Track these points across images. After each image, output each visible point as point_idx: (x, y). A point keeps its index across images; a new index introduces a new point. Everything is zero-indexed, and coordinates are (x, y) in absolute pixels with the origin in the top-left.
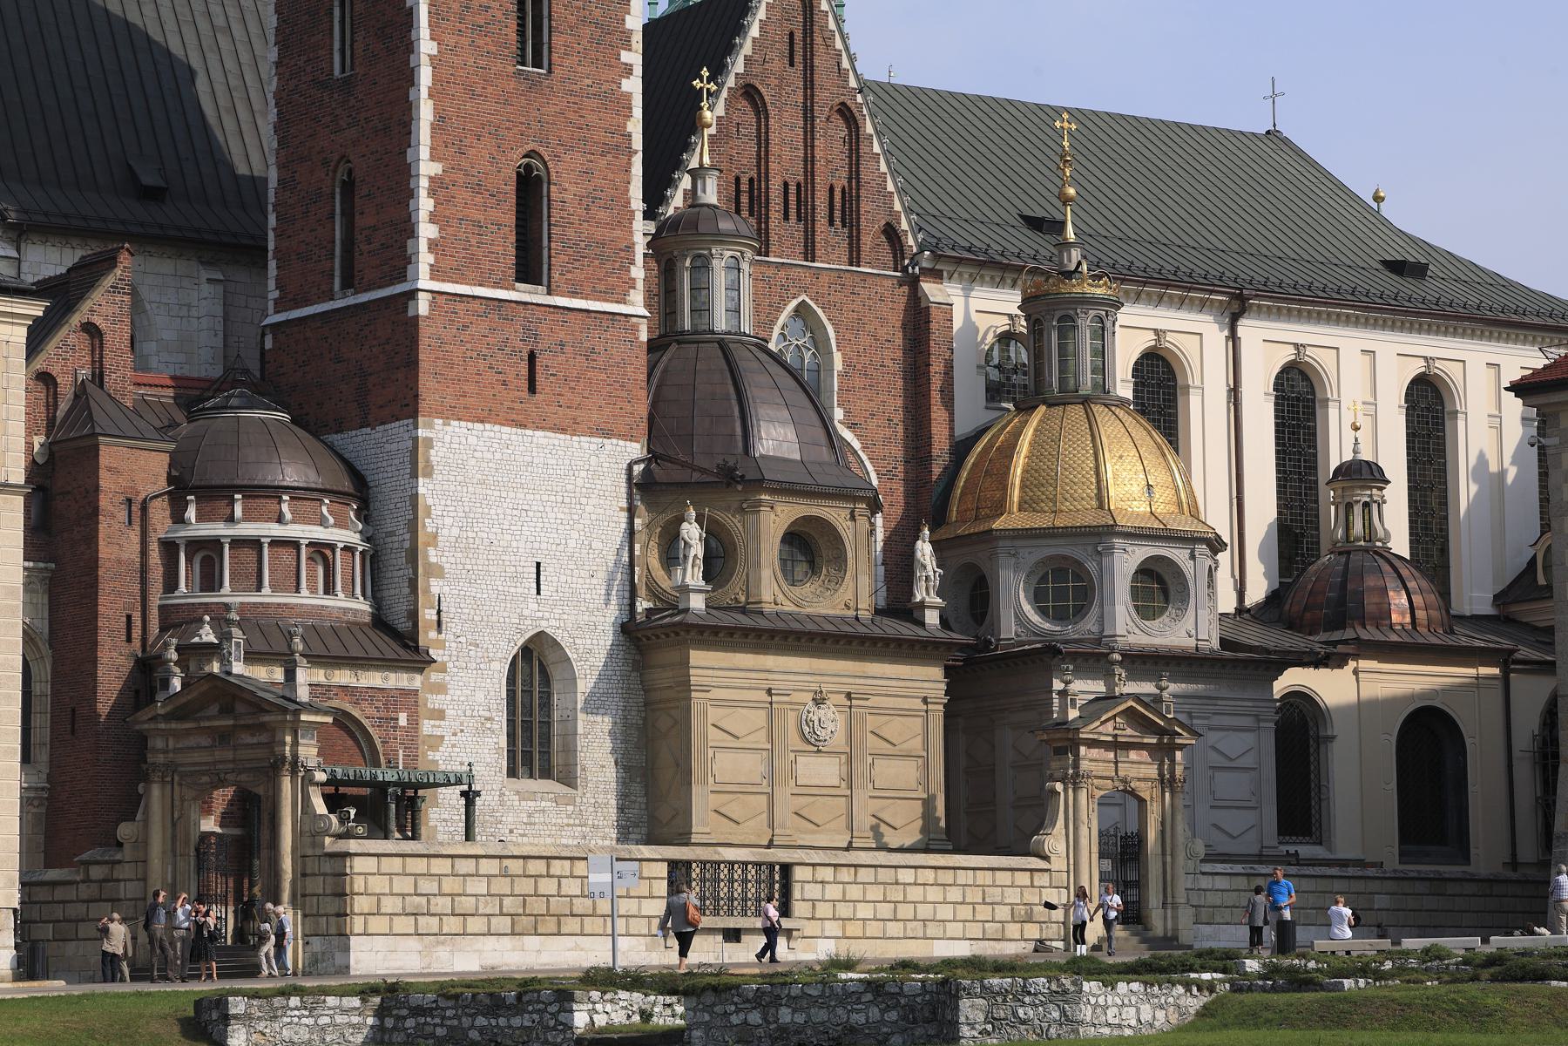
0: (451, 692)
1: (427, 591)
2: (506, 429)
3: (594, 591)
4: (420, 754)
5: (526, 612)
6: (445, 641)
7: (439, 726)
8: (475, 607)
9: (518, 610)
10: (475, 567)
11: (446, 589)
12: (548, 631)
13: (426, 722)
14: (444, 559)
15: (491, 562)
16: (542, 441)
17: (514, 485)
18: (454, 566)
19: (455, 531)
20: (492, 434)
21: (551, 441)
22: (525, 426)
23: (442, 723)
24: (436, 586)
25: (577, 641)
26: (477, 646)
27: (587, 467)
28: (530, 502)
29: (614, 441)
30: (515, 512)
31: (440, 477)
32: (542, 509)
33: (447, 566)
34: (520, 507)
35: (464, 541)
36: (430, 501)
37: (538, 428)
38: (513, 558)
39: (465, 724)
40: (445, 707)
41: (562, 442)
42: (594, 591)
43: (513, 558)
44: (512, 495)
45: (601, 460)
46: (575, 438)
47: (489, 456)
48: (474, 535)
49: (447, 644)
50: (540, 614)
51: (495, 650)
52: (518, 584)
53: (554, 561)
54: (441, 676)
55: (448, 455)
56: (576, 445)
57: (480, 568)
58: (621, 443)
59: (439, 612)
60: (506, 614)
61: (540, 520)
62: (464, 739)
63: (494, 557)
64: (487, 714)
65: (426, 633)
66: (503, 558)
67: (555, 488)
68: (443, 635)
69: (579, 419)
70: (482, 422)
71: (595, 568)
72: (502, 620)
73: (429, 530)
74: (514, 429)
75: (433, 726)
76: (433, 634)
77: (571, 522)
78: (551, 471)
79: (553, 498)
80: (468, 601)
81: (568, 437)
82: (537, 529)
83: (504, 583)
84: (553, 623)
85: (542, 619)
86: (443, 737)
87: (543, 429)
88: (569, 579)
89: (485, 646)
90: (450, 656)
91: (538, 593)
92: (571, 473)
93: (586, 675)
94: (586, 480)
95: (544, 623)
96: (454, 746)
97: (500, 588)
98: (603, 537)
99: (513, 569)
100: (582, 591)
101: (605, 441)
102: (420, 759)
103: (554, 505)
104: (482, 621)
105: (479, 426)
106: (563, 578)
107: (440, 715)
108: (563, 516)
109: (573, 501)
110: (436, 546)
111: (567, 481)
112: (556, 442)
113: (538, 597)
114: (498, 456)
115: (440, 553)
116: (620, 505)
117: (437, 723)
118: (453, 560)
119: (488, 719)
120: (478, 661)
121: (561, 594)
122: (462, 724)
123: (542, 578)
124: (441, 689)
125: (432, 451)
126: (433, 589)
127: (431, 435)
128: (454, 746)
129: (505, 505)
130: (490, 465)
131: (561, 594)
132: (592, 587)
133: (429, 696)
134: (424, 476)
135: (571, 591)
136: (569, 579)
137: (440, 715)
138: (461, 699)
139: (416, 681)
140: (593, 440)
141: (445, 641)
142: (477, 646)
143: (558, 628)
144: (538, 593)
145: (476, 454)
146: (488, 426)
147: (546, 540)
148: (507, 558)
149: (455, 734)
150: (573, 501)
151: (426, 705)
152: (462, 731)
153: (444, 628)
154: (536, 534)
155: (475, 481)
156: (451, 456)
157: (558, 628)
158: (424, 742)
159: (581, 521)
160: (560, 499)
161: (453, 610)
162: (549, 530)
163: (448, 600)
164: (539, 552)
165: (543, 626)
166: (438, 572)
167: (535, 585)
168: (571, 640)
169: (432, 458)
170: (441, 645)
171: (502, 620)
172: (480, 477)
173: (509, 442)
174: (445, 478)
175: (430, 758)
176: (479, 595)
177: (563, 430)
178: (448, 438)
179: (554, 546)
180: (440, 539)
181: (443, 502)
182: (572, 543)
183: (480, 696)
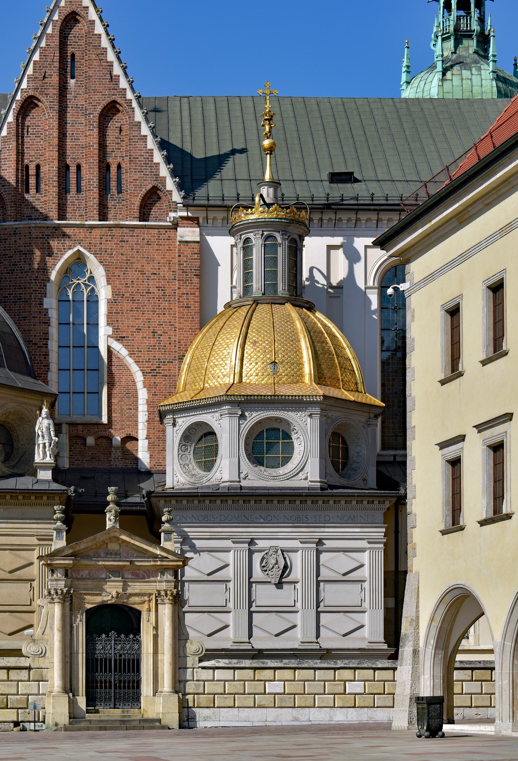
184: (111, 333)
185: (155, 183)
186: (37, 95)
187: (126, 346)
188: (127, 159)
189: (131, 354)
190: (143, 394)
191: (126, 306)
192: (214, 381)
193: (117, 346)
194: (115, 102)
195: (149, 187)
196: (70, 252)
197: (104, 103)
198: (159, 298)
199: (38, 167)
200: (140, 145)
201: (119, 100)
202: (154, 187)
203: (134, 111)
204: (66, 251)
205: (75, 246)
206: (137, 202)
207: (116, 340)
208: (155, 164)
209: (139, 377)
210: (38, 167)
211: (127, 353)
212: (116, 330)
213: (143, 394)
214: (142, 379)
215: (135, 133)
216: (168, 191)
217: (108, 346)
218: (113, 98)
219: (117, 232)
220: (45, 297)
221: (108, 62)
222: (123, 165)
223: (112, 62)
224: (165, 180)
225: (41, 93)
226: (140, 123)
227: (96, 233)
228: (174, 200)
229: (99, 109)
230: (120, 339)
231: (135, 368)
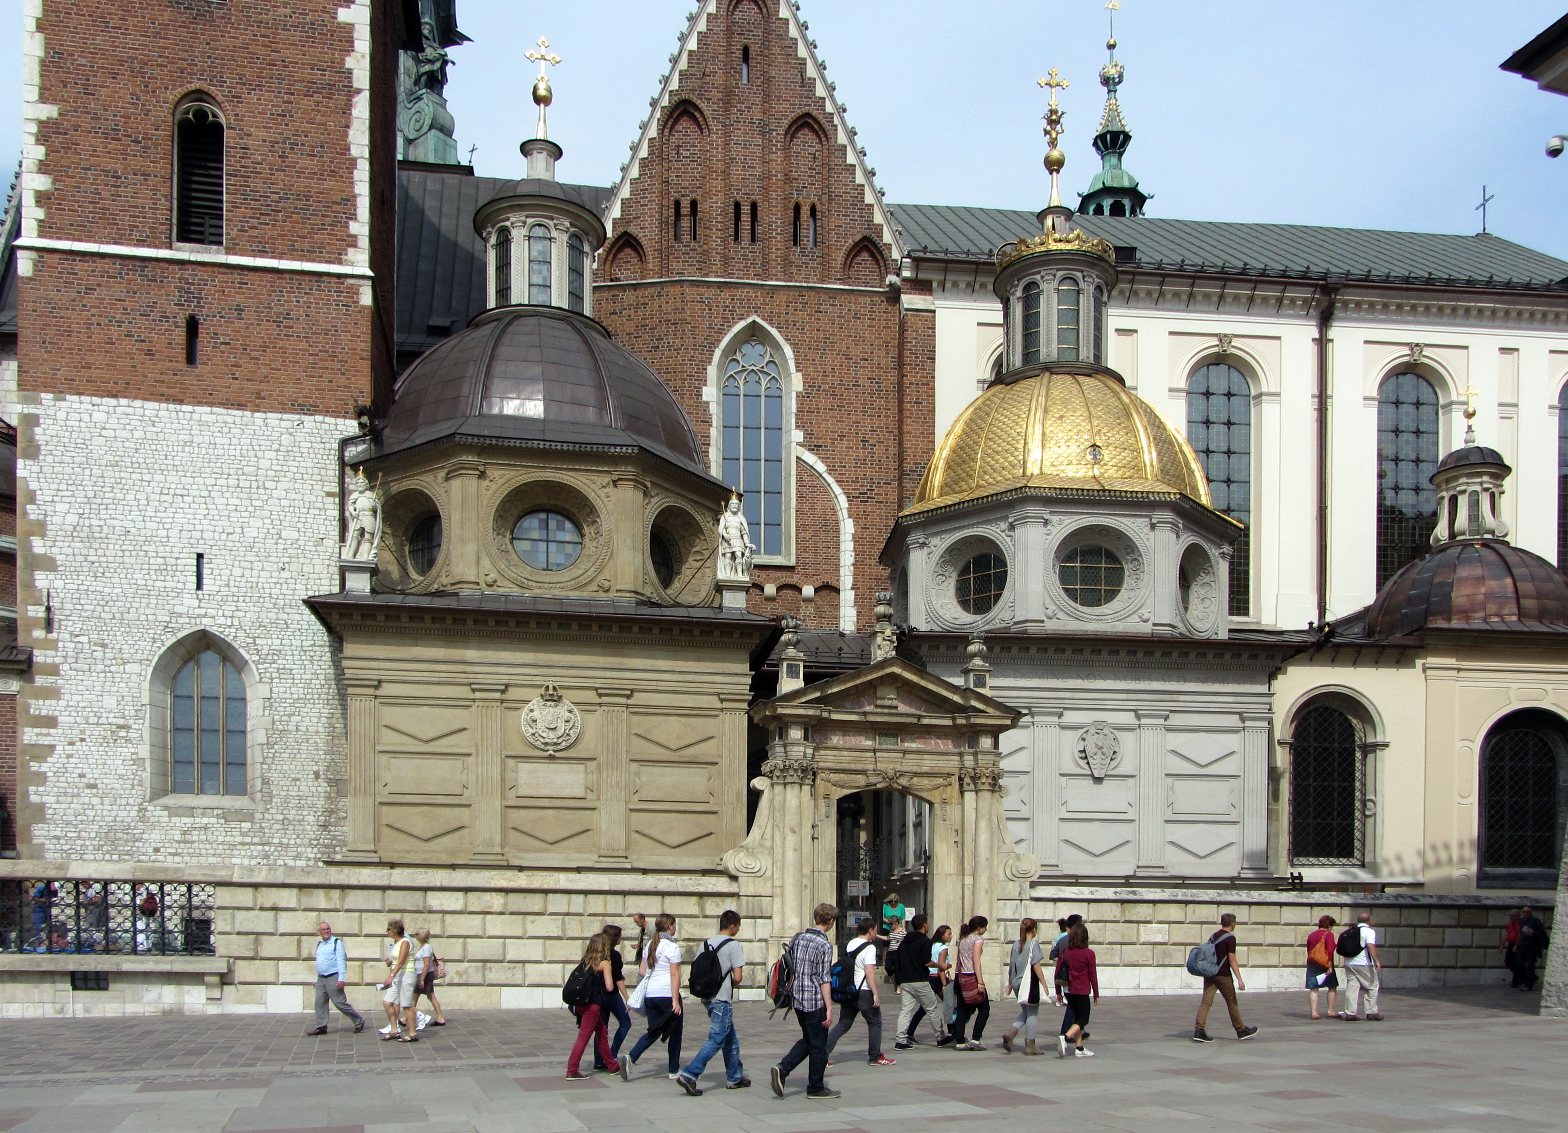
0: (67, 697)
1: (30, 585)
2: (155, 405)
3: (285, 586)
4: (18, 764)
5: (178, 609)
6: (57, 641)
7: (48, 735)
8: (102, 603)
9: (167, 607)
10: (104, 559)
11: (59, 583)
12: (214, 630)
13: (27, 730)
14: (54, 550)
15: (127, 553)
16: (205, 418)
17: (163, 467)
18: (71, 558)
19: (72, 519)
20: (130, 410)
21: (220, 418)
22: (181, 402)
23: (52, 731)
24: (42, 580)
25: (258, 641)
26: (104, 646)
27: (275, 447)
28: (187, 487)
29: (319, 418)
30: (164, 498)
31: (49, 459)
32: (206, 494)
33: (58, 557)
34: (171, 491)
35: (86, 529)
36: (33, 486)
37: (200, 403)
38: (161, 549)
39: (88, 733)
40: (57, 713)
41: (238, 420)
42: (285, 586)
43: (161, 549)
44: (159, 477)
45: (298, 439)
46: (257, 415)
47: (125, 434)
48: (102, 523)
49: (60, 644)
50: (203, 611)
51: (132, 651)
52: (169, 578)
53: (223, 552)
54: (51, 679)
55: (61, 434)
56: (259, 422)
57: (110, 559)
58: (328, 419)
59: (48, 609)
60: (148, 611)
61: (204, 506)
62: (85, 748)
63: (131, 548)
64: (121, 722)
65: (29, 632)
66: (145, 548)
67: (226, 471)
68: (54, 635)
69: (263, 394)
70: (115, 396)
71: (287, 560)
72: (143, 617)
73: (33, 517)
74: (164, 406)
75: (37, 735)
76: (39, 633)
77: (251, 509)
78: (221, 452)
79: (224, 482)
80: (93, 597)
81: (248, 413)
82: (198, 517)
83: (147, 577)
84: (222, 621)
85: (205, 616)
86: (52, 748)
87: (211, 404)
88: (247, 573)
89: (117, 646)
90: (65, 657)
91: (199, 586)
92: (252, 453)
93: (272, 679)
94: (275, 462)
95: (205, 621)
96: (69, 756)
97: (140, 582)
98: (300, 525)
99: (162, 561)
100: (266, 586)
101: (305, 418)
102: (18, 770)
103: (225, 489)
104: (114, 618)
105: (112, 401)
106: (237, 572)
107: (51, 722)
108: (238, 502)
109: (255, 485)
110: (43, 535)
111: (244, 463)
112: (230, 419)
113: (199, 592)
114: (138, 434)
115: (50, 544)
116: (326, 489)
117: (44, 731)
118: (70, 551)
119: (121, 727)
120: (108, 662)
121: (233, 589)
122: (83, 732)
123: (206, 571)
124: (53, 693)
125: (37, 430)
126: (37, 583)
127: (37, 412)
128: (69, 756)
129: (149, 490)
130: (126, 444)
131: (233, 589)
132: (281, 581)
133: (32, 702)
134: (26, 457)
135: (249, 585)
136: (247, 573)
137: (51, 722)
138: (81, 704)
139: (14, 686)
140: (285, 416)
141: (57, 641)
142: (104, 646)
143: (230, 627)
144: (199, 586)
145: (104, 432)
146: (124, 401)
147: (211, 528)
148: (153, 548)
149: (72, 744)
150: (255, 485)
151: (27, 711)
152: (83, 740)
153: (56, 625)
154: (197, 522)
155: (104, 462)
156: (67, 434)
157: (230, 627)
158: (24, 753)
159: (266, 507)
160: (232, 482)
161: (70, 606)
162: (217, 518)
163: (62, 595)
164: (201, 542)
165: (206, 624)
166: (49, 564)
167: (194, 579)
168: (251, 640)
169: (37, 437)
170: (53, 645)
171: (143, 617)
172: (111, 458)
173: (156, 419)
174: (57, 459)
175: (33, 769)
176: (107, 590)
177: (241, 406)
178: (61, 415)
179: (224, 536)
180: (50, 527)
181: (54, 486)
182: (251, 533)
183: (110, 702)
184: (801, 440)
185: (866, 233)
186: (694, 99)
187: (824, 460)
188: (825, 198)
189: (830, 471)
190: (848, 528)
191: (824, 402)
192: (996, 475)
193: (810, 458)
194: (808, 115)
195: (858, 237)
196: (742, 324)
197: (792, 116)
198: (872, 394)
199: (694, 204)
200: (844, 177)
201: (815, 113)
202: (865, 238)
203: (836, 130)
204: (736, 323)
205: (748, 316)
206: (839, 257)
207: (809, 450)
208: (867, 205)
209: (843, 502)
210: (694, 204)
211: (825, 468)
212: (808, 435)
213: (848, 528)
214: (847, 505)
215: (837, 161)
216: (885, 244)
217: (797, 458)
218: (806, 109)
219: (808, 296)
220: (705, 385)
221: (798, 59)
222: (819, 207)
223: (804, 59)
224: (882, 230)
225: (700, 97)
226: (845, 147)
227: (781, 298)
228: (894, 257)
229: (785, 123)
230: (814, 448)
231: (837, 489)
